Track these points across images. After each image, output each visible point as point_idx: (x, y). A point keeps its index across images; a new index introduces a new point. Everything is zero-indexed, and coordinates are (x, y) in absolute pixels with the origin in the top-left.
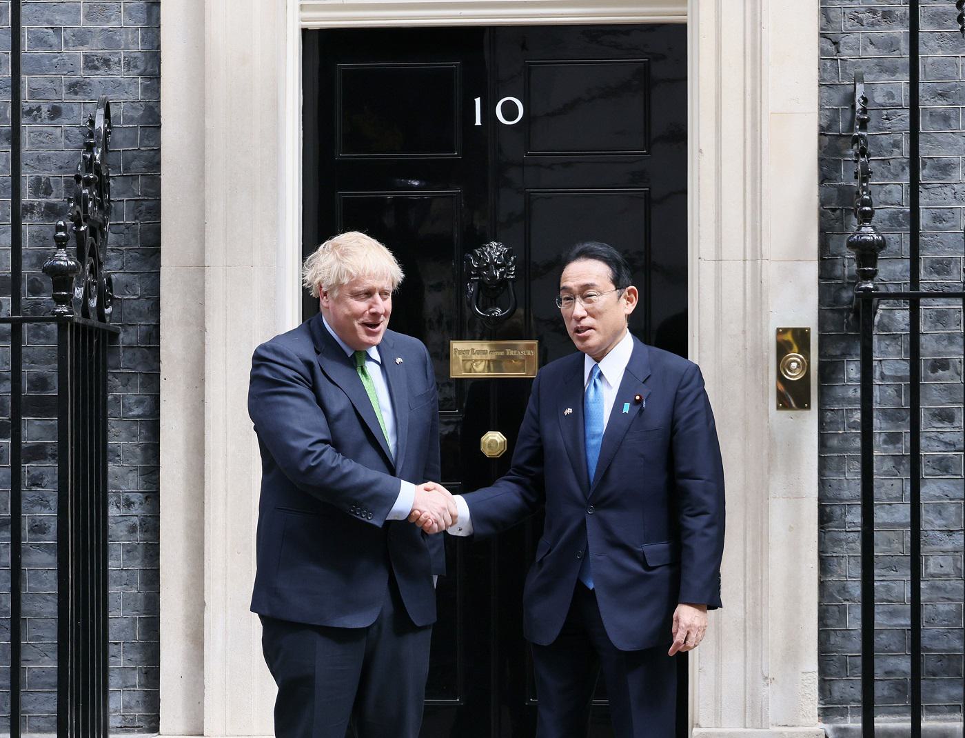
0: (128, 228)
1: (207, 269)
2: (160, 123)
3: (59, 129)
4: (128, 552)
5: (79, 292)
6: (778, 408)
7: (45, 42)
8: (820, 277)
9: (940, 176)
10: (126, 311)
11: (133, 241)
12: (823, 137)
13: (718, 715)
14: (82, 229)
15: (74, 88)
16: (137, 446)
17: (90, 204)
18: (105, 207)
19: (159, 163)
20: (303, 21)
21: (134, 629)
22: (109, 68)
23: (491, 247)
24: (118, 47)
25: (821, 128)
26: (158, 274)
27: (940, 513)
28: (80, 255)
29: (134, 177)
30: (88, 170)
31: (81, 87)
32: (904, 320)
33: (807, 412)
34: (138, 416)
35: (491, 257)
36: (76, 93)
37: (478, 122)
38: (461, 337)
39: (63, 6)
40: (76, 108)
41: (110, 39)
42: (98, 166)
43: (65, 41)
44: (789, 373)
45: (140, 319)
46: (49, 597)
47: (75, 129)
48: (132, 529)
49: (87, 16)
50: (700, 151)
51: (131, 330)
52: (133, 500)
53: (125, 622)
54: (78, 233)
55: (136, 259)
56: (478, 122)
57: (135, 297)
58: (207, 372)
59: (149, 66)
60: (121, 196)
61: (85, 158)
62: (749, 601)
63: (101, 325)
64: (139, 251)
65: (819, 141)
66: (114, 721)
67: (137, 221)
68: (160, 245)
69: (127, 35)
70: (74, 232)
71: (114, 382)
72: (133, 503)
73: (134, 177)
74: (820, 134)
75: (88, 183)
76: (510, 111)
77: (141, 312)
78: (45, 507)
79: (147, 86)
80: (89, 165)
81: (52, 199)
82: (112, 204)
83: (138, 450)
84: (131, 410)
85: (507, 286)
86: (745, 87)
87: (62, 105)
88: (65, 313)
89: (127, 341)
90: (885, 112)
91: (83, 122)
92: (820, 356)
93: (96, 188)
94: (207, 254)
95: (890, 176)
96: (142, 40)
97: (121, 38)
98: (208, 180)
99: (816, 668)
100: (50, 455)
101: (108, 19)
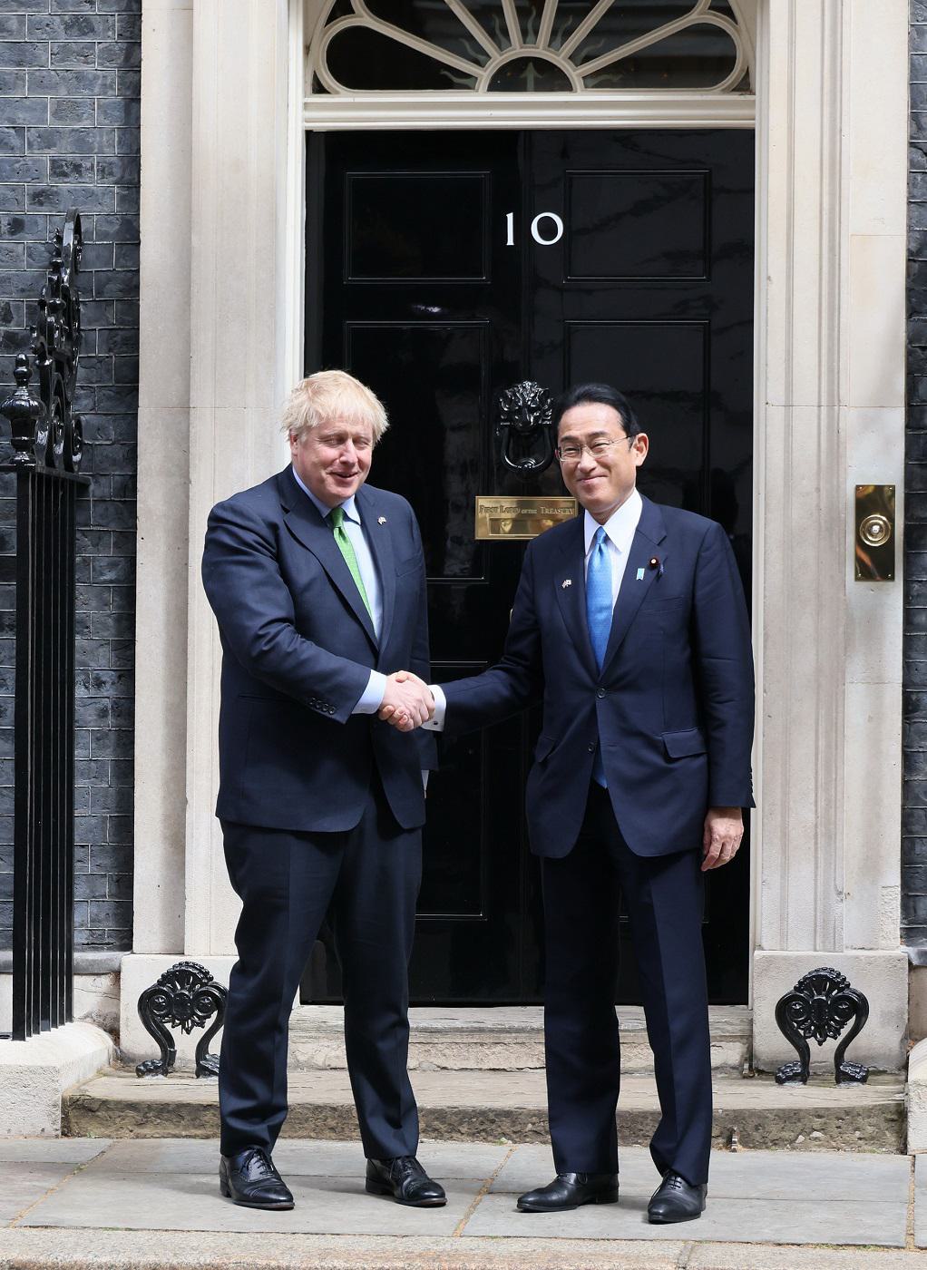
1: (192, 411)
3: (21, 246)
4: (98, 739)
5: (42, 437)
6: (857, 579)
7: (6, 144)
8: (907, 426)
10: (97, 459)
11: (106, 377)
12: (913, 263)
13: (783, 936)
14: (47, 363)
15: (39, 197)
16: (109, 616)
17: (57, 334)
18: (74, 338)
19: (137, 287)
20: (306, 122)
21: (103, 830)
22: (81, 175)
23: (524, 388)
24: (91, 150)
26: (135, 416)
28: (44, 394)
29: (109, 303)
30: (54, 295)
31: (47, 196)
33: (890, 583)
34: (111, 582)
35: (524, 399)
36: (41, 204)
37: (510, 242)
38: (488, 492)
39: (27, 102)
40: (41, 221)
41: (81, 141)
42: (66, 289)
43: (29, 143)
44: (870, 538)
45: (114, 468)
46: (5, 792)
47: (39, 246)
48: (103, 714)
49: (54, 114)
50: (769, 278)
51: (103, 480)
52: (104, 679)
53: (93, 821)
54: (42, 368)
55: (109, 398)
56: (510, 242)
57: (108, 443)
58: (191, 530)
59: (128, 171)
60: (93, 324)
61: (51, 280)
62: (822, 804)
63: (68, 475)
64: (113, 389)
65: (908, 268)
66: (79, 937)
67: (112, 354)
69: (101, 137)
70: (38, 366)
72: (104, 683)
73: (109, 303)
74: (909, 260)
76: (548, 229)
77: (115, 460)
79: (124, 196)
80: (56, 288)
81: (13, 328)
82: (83, 334)
83: (110, 622)
84: (102, 574)
85: (543, 432)
86: (821, 204)
88: (26, 462)
89: (99, 493)
91: (50, 237)
92: (907, 518)
93: (64, 315)
96: (119, 142)
97: (95, 140)
98: (194, 306)
99: (898, 882)
101: (79, 118)
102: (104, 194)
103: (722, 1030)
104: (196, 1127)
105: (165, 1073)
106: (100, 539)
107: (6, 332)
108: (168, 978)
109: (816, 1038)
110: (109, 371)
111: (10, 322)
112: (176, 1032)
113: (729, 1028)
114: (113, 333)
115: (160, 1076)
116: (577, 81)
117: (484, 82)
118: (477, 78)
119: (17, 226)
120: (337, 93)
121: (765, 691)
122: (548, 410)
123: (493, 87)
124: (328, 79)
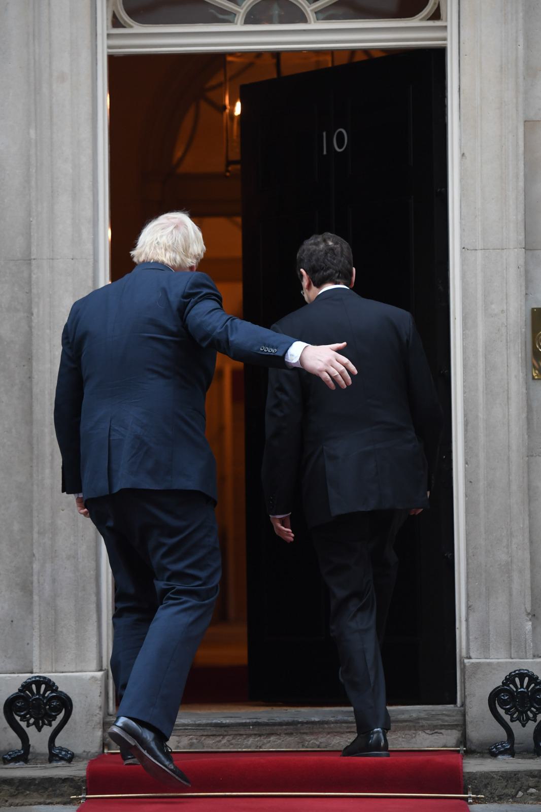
1: (33, 262)
94: (34, 249)
103: (443, 720)
104: (57, 796)
105: (26, 761)
108: (26, 686)
109: (520, 721)
112: (31, 731)
113: (447, 718)
115: (21, 763)
116: (311, 16)
117: (240, 18)
118: (235, 15)
120: (131, 27)
121: (466, 463)
123: (247, 21)
124: (124, 16)
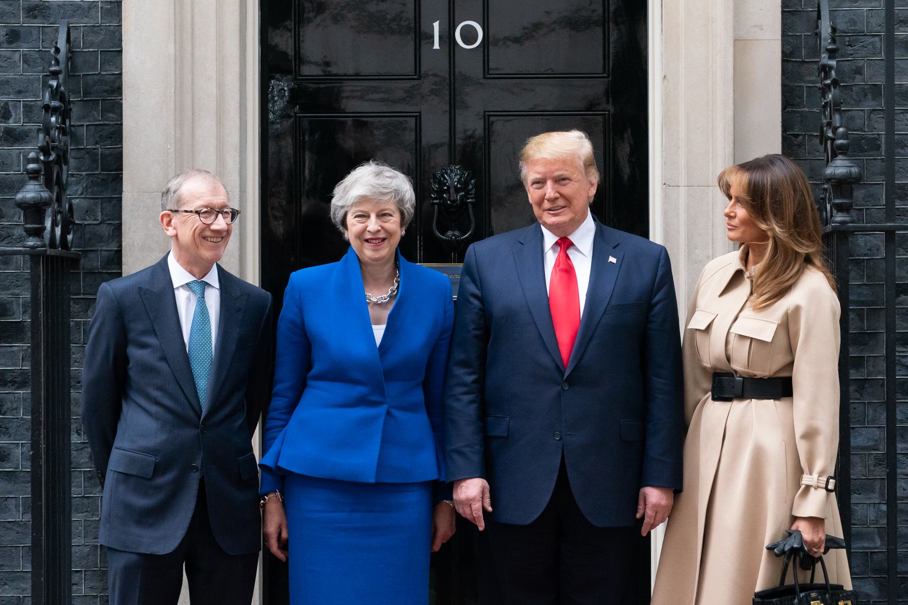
0: (88, 153)
2: (120, 46)
3: (16, 56)
4: (90, 478)
5: (48, 224)
9: (902, 102)
14: (51, 158)
15: (33, 11)
19: (119, 90)
23: (451, 171)
25: (784, 54)
27: (902, 436)
28: (48, 185)
32: (866, 245)
36: (35, 17)
37: (436, 46)
40: (35, 32)
46: (9, 525)
51: (92, 255)
53: (87, 550)
56: (436, 46)
57: (95, 222)
64: (100, 177)
67: (98, 146)
68: (122, 170)
70: (43, 162)
71: (75, 308)
75: (55, 111)
76: (469, 35)
78: (5, 434)
79: (107, 10)
81: (11, 124)
85: (467, 208)
87: (21, 29)
90: (847, 39)
95: (852, 102)
100: (10, 382)
102: (90, 8)
106: (89, 306)
107: (5, 128)
110: (96, 161)
111: (9, 119)
114: (99, 128)
119: (14, 36)
122: (472, 189)
